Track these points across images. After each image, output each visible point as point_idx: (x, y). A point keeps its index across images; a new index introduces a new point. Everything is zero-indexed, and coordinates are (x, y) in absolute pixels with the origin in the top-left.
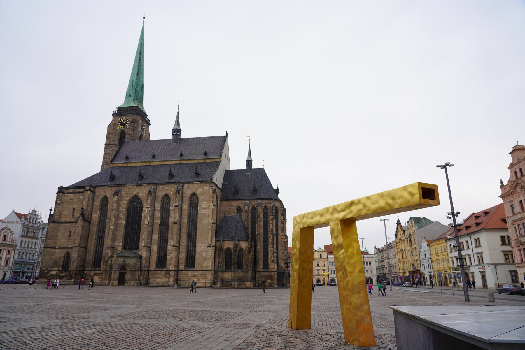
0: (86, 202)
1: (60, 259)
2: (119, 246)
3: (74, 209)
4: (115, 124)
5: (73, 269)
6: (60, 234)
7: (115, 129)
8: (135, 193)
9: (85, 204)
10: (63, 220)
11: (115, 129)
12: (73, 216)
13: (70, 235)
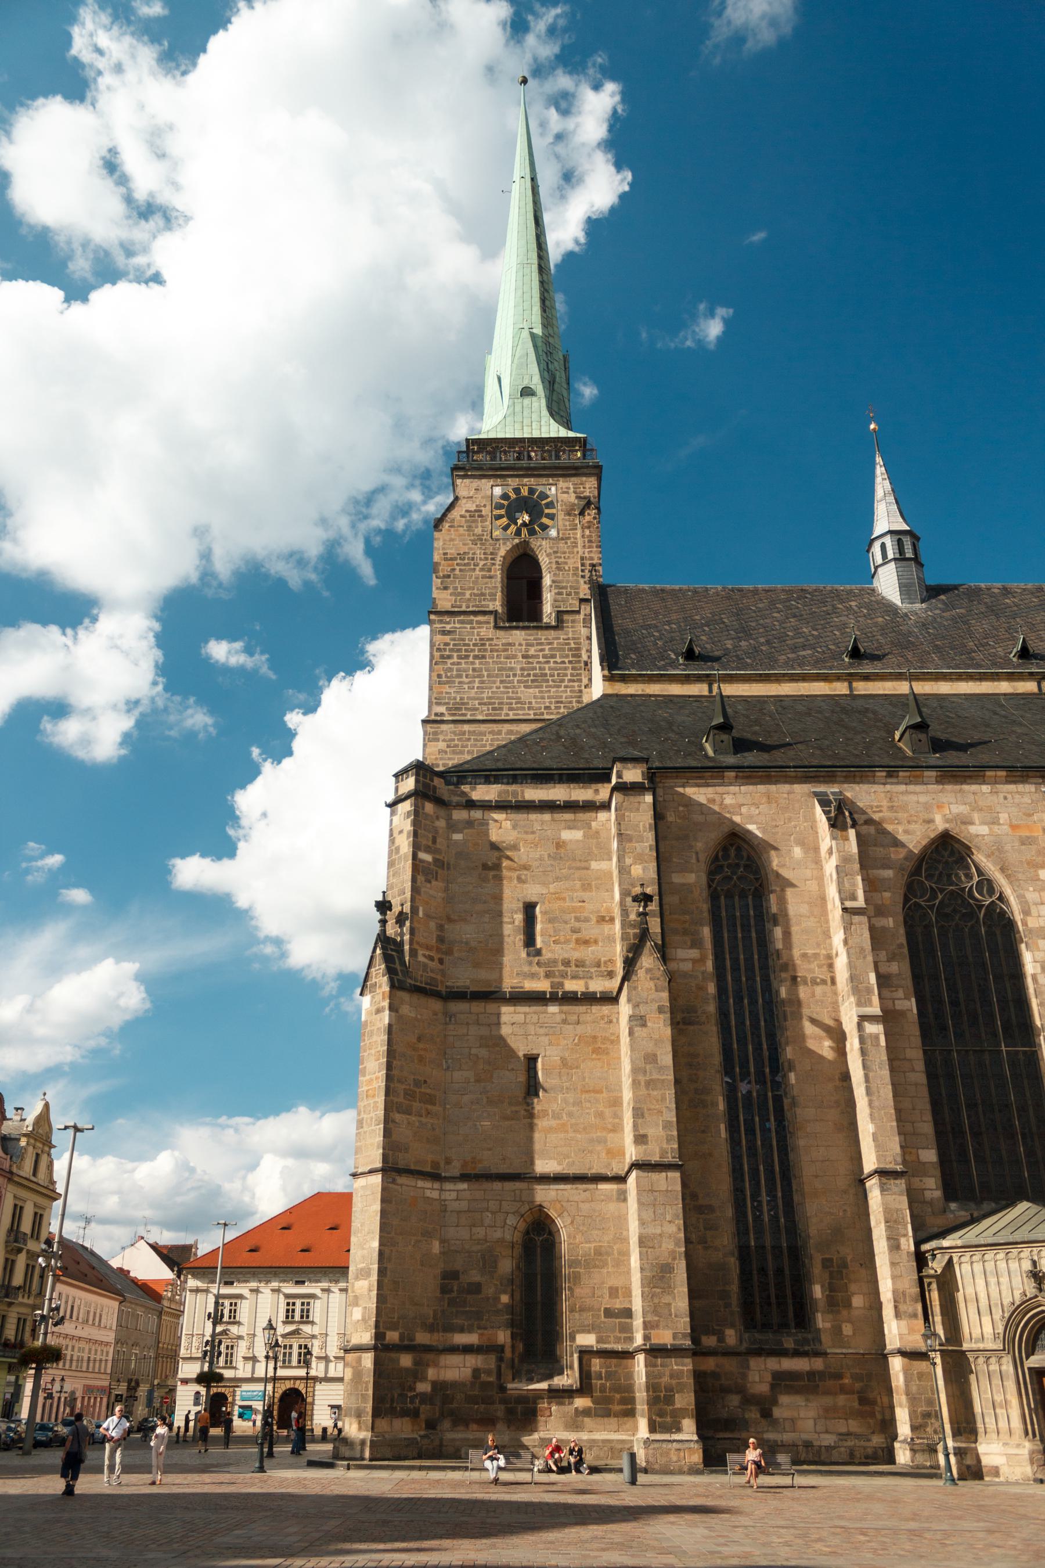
0: (639, 859)
1: (488, 1261)
7: (478, 540)
8: (940, 825)
9: (637, 871)
11: (478, 540)
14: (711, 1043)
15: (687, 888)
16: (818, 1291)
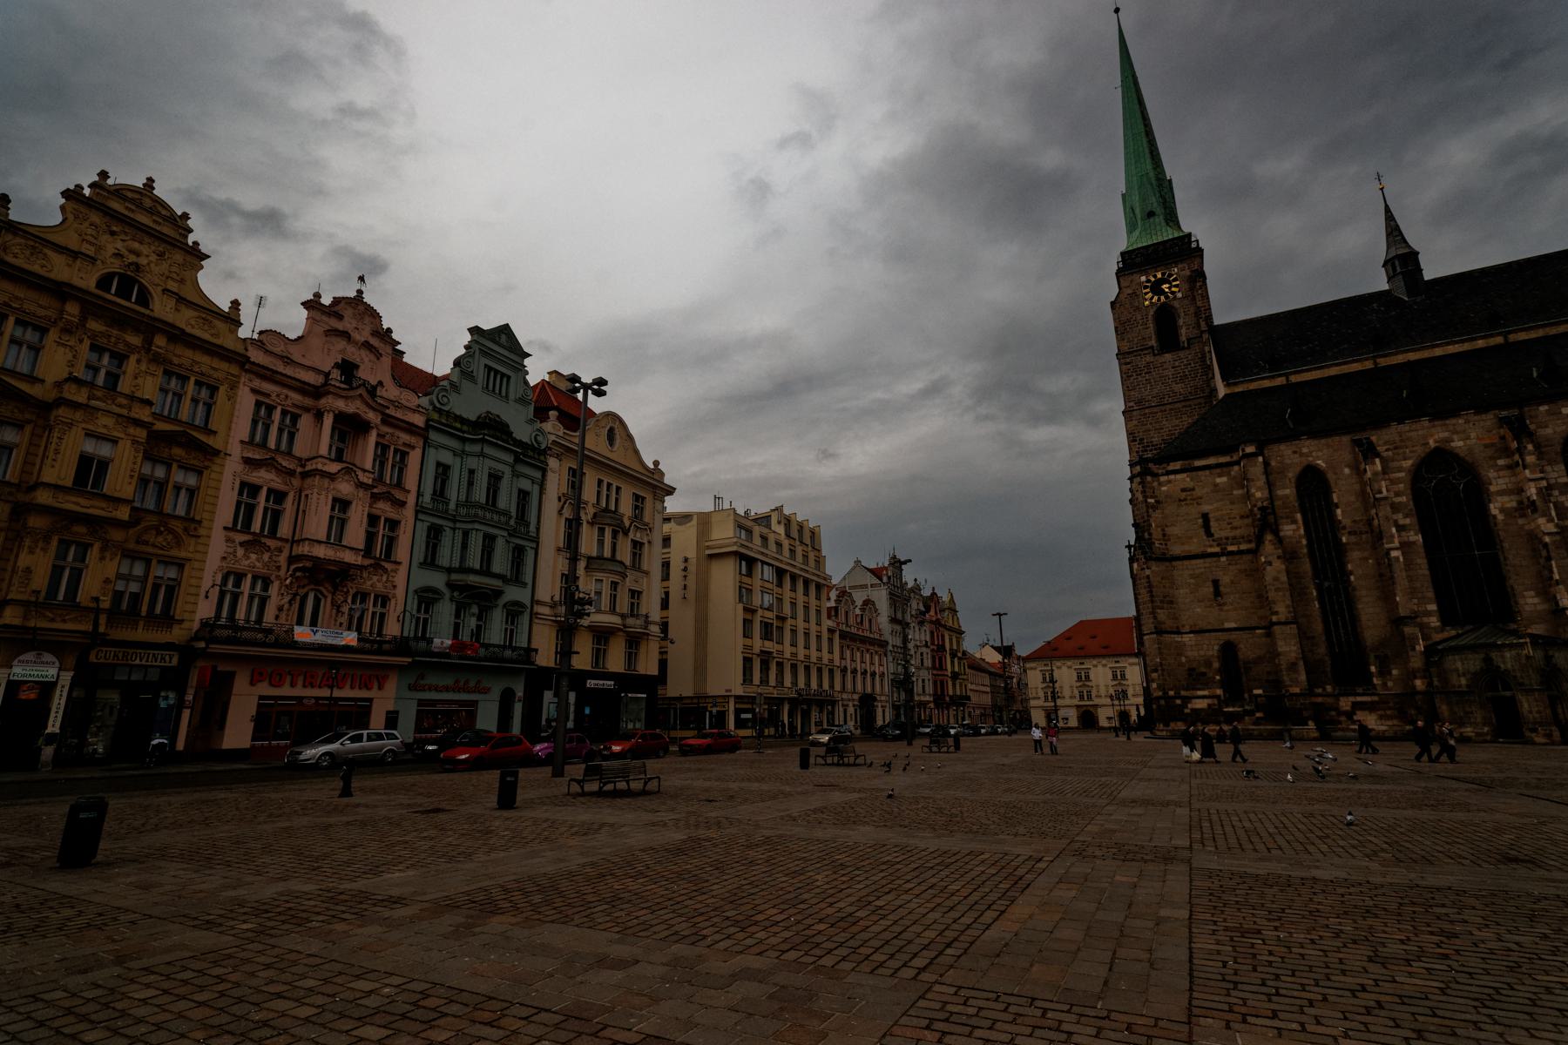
0: (1259, 489)
1: (1208, 663)
2: (1429, 614)
3: (1205, 517)
4: (1134, 295)
5: (1297, 690)
6: (1182, 593)
10: (1176, 550)
12: (1209, 534)
13: (1217, 593)
14: (1307, 566)
15: (1287, 497)
16: (1373, 669)
